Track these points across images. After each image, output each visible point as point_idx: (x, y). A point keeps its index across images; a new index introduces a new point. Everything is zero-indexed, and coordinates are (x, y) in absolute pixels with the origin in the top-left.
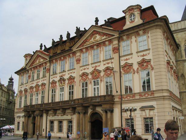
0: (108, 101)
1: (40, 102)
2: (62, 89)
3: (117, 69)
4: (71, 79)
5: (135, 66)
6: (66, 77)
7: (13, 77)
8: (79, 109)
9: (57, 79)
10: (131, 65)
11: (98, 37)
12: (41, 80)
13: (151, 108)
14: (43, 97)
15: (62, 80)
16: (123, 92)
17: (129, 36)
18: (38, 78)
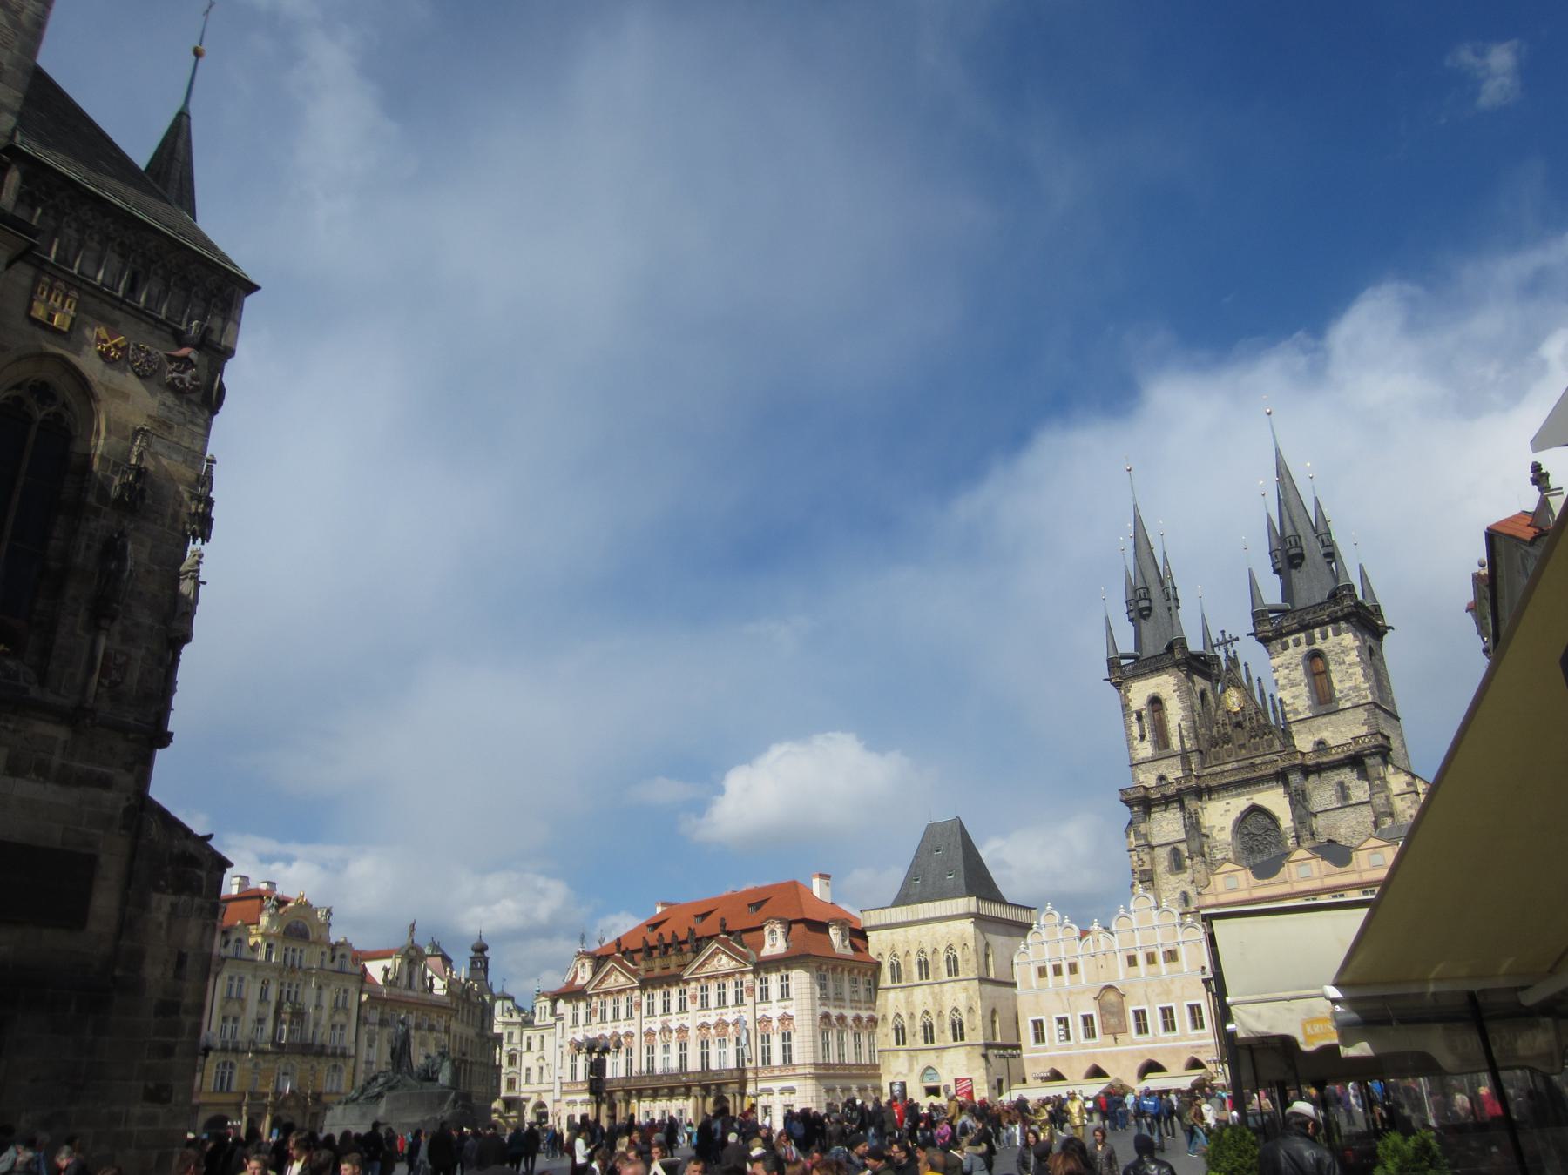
0: (740, 1077)
1: (622, 1073)
2: (666, 1048)
3: (750, 1025)
4: (683, 1030)
5: (775, 1023)
6: (674, 1025)
7: (485, 941)
8: (696, 1090)
9: (657, 1027)
10: (769, 1020)
11: (725, 959)
12: (622, 1023)
13: (792, 1090)
14: (629, 1063)
15: (666, 1029)
16: (760, 1064)
17: (768, 971)
18: (616, 1017)
